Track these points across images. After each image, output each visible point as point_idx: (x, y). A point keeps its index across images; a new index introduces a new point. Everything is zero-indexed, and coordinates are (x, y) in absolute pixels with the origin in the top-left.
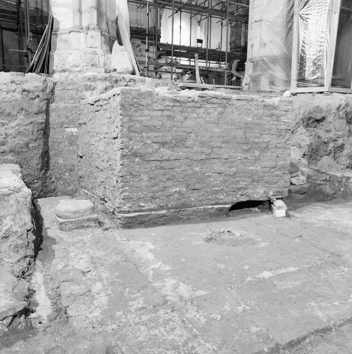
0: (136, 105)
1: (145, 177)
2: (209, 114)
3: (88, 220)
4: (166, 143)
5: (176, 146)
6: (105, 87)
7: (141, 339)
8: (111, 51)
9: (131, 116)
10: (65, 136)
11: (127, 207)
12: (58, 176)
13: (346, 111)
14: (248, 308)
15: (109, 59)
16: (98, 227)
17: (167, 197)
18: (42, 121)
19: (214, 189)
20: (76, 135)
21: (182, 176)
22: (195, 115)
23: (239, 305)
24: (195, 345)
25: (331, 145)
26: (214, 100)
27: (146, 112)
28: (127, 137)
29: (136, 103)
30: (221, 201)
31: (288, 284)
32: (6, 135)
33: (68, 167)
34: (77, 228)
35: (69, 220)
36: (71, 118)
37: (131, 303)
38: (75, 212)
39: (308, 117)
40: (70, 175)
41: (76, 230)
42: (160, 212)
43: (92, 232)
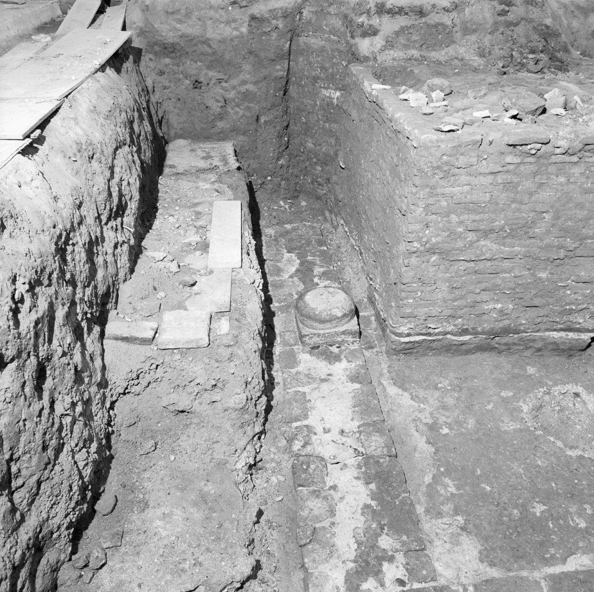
0: (445, 168)
1: (444, 287)
5: (511, 235)
9: (433, 188)
10: (318, 103)
11: (406, 329)
16: (358, 342)
17: (478, 316)
18: (282, 73)
19: (568, 307)
20: (337, 105)
21: (512, 285)
28: (422, 222)
29: (446, 163)
30: (578, 326)
32: (225, 101)
35: (316, 332)
36: (330, 71)
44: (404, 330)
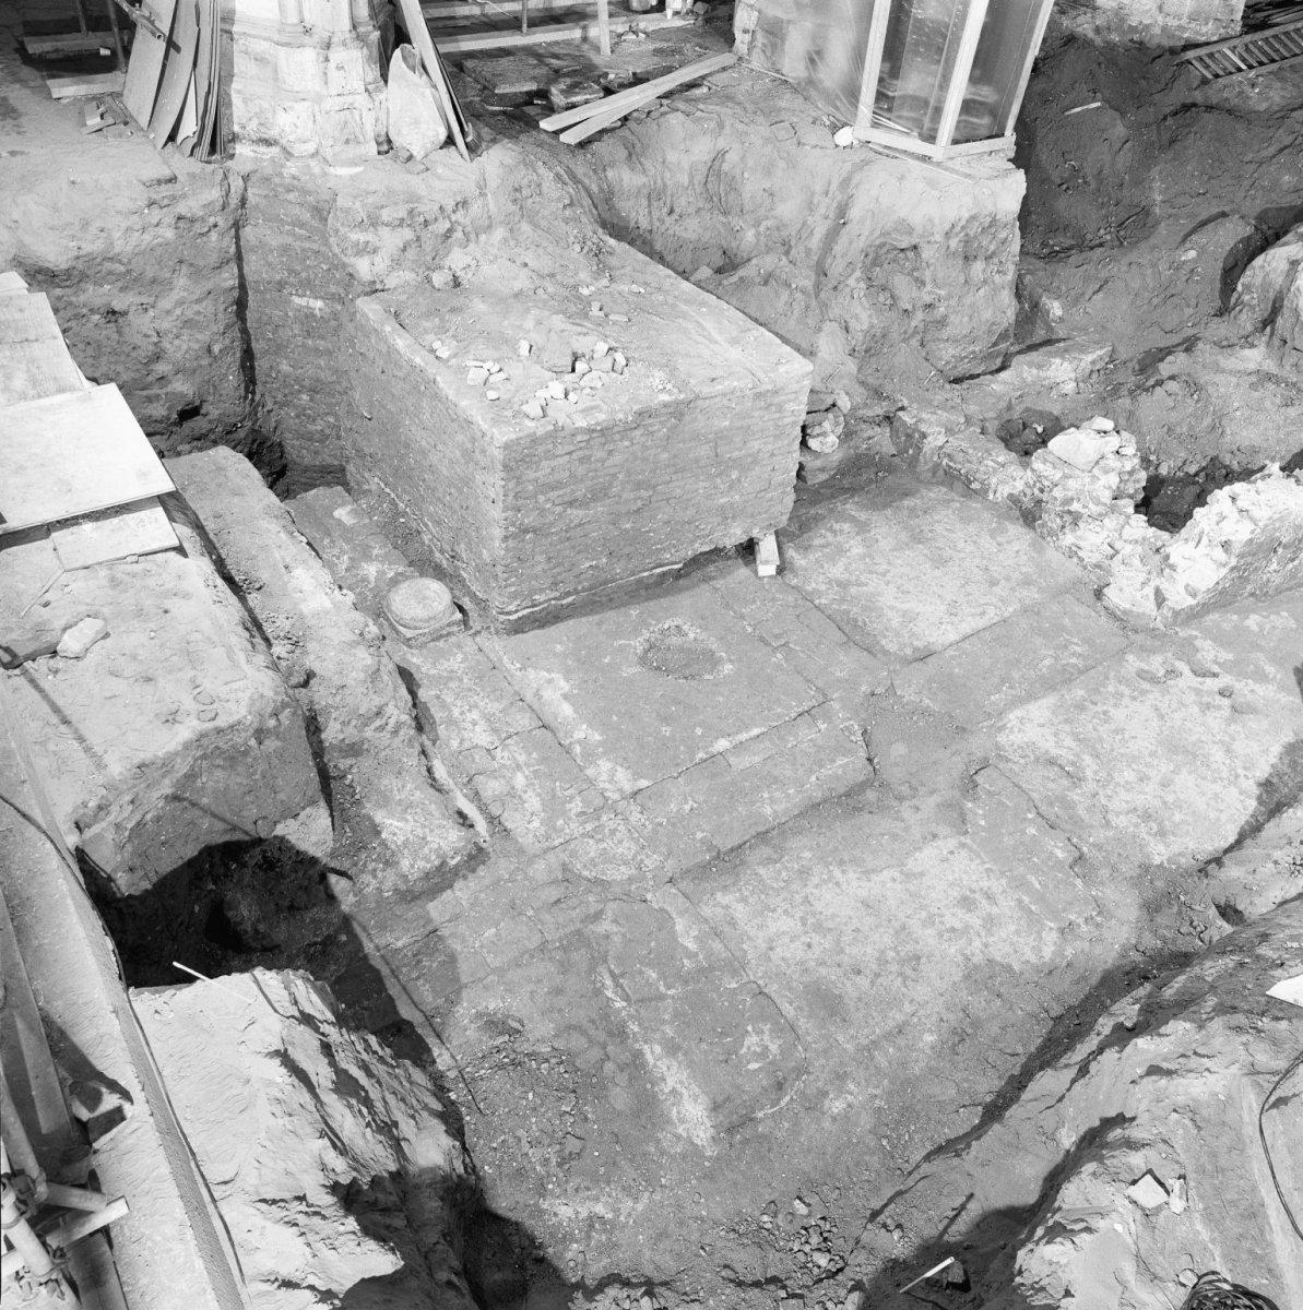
1: (541, 558)
5: (593, 500)
6: (401, 246)
7: (592, 854)
8: (384, 77)
10: (290, 314)
12: (280, 397)
13: (967, 235)
22: (627, 443)
23: (686, 802)
25: (920, 315)
26: (664, 411)
27: (544, 463)
31: (740, 762)
34: (433, 640)
36: (304, 275)
37: (568, 806)
38: (430, 618)
39: (877, 243)
40: (311, 400)
42: (564, 602)
43: (459, 647)
44: (512, 608)
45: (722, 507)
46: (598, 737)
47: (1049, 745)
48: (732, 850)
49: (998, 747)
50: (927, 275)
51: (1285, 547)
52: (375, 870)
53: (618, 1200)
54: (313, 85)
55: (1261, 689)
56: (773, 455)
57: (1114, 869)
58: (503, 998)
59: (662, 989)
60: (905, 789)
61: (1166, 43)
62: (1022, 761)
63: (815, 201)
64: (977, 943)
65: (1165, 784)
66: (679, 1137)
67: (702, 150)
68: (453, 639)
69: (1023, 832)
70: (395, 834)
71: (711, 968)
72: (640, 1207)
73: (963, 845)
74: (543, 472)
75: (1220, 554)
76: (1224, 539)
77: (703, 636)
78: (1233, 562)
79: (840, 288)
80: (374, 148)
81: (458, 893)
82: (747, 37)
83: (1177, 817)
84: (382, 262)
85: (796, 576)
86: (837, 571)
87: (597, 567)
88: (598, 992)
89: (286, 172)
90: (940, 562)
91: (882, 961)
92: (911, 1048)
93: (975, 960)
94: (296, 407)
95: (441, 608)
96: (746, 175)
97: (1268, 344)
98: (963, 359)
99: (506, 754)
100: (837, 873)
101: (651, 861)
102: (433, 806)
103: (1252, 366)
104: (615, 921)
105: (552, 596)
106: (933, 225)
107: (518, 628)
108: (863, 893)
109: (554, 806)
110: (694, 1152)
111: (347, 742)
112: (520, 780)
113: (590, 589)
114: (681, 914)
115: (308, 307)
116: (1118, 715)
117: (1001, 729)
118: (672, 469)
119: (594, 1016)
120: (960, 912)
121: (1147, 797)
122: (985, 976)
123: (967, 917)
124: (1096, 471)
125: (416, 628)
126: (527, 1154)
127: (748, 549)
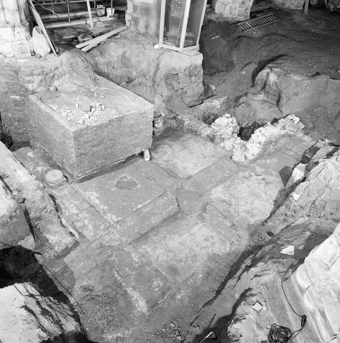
1: (86, 161)
2: (113, 126)
3: (63, 182)
4: (95, 145)
5: (99, 145)
6: (40, 80)
7: (108, 239)
8: (31, 35)
9: (79, 140)
10: (10, 100)
12: (9, 123)
14: (134, 223)
15: (32, 43)
22: (107, 129)
23: (132, 222)
24: (122, 238)
25: (180, 91)
27: (85, 136)
31: (145, 210)
33: (16, 119)
34: (59, 186)
36: (13, 89)
37: (100, 227)
39: (167, 73)
40: (18, 124)
41: (59, 187)
43: (66, 187)
44: (80, 175)
45: (134, 143)
46: (106, 208)
47: (223, 197)
48: (145, 233)
49: (210, 199)
50: (181, 81)
51: (274, 142)
52: (48, 251)
53: (124, 331)
54: (11, 38)
55: (272, 178)
56: (146, 129)
57: (242, 226)
58: (87, 281)
59: (130, 273)
60: (188, 212)
61: (232, 21)
62: (217, 202)
63: (151, 63)
64: (210, 250)
65: (252, 204)
66: (139, 311)
67: (120, 51)
68: (64, 185)
69: (219, 220)
70: (53, 241)
71: (143, 266)
72: (130, 332)
73: (204, 225)
74: (85, 138)
75: (258, 145)
76: (259, 141)
77: (132, 178)
78: (262, 147)
79: (159, 85)
80: (30, 55)
81: (72, 255)
82: (129, 22)
83: (256, 212)
84: (35, 85)
85: (155, 160)
86: (165, 158)
87: (102, 162)
88: (113, 276)
89: (5, 62)
90: (191, 153)
91: (187, 258)
92: (196, 279)
93: (210, 254)
94: (14, 126)
95: (60, 177)
96: (132, 58)
97: (264, 93)
98: (192, 101)
99: (82, 215)
100: (173, 236)
101: (124, 239)
102: (63, 232)
103: (261, 99)
104: (116, 257)
105: (91, 171)
106: (181, 68)
107: (82, 181)
108: (180, 241)
109: (96, 228)
110: (143, 315)
111: (37, 217)
112: (86, 222)
113: (101, 169)
114: (133, 252)
115: (15, 99)
116: (239, 187)
117: (210, 194)
118: (120, 135)
119: (113, 282)
120: (205, 242)
121: (248, 207)
122: (213, 258)
123: (207, 243)
124: (227, 127)
125: (54, 183)
126: (98, 323)
127: (142, 154)
